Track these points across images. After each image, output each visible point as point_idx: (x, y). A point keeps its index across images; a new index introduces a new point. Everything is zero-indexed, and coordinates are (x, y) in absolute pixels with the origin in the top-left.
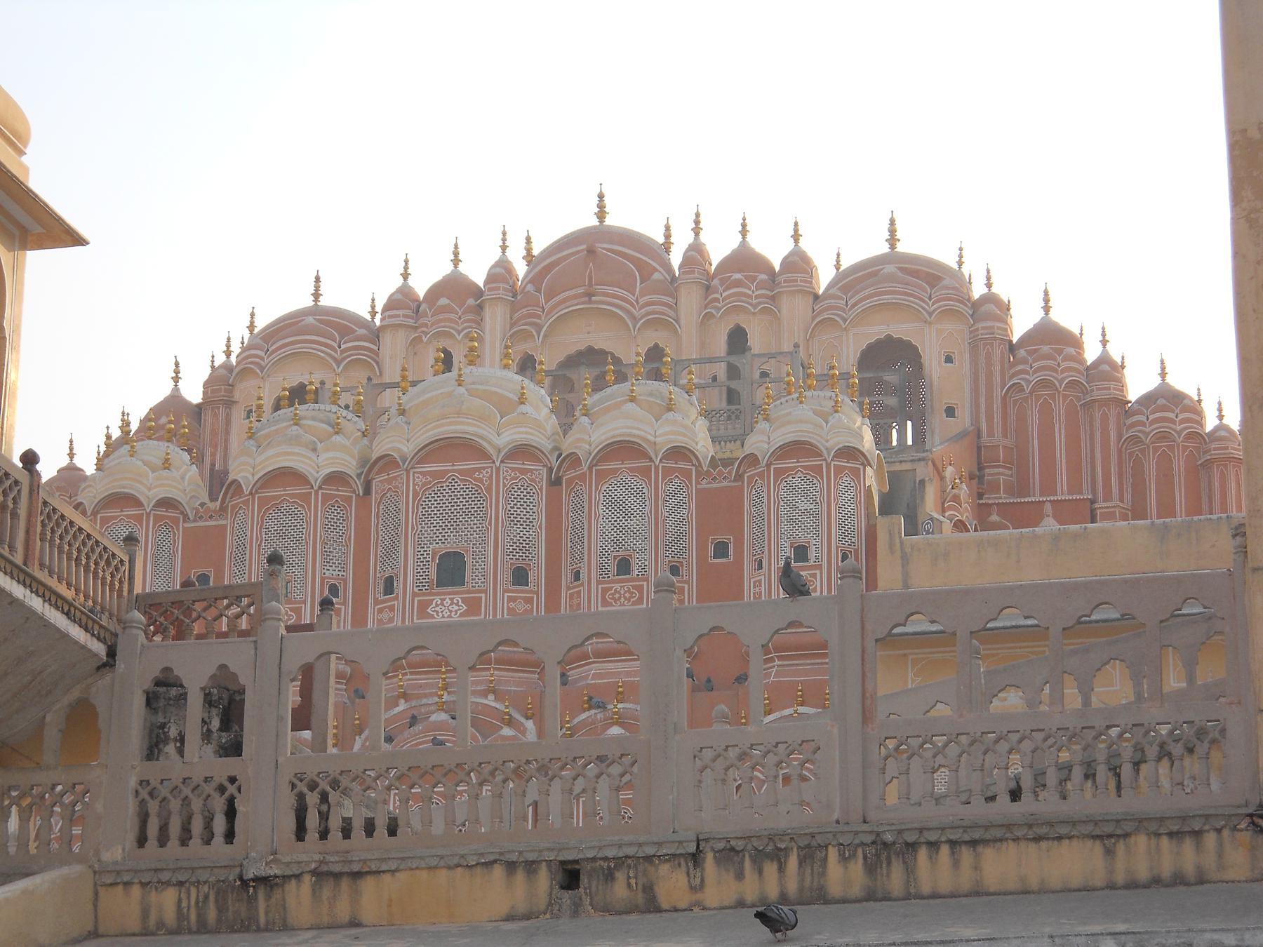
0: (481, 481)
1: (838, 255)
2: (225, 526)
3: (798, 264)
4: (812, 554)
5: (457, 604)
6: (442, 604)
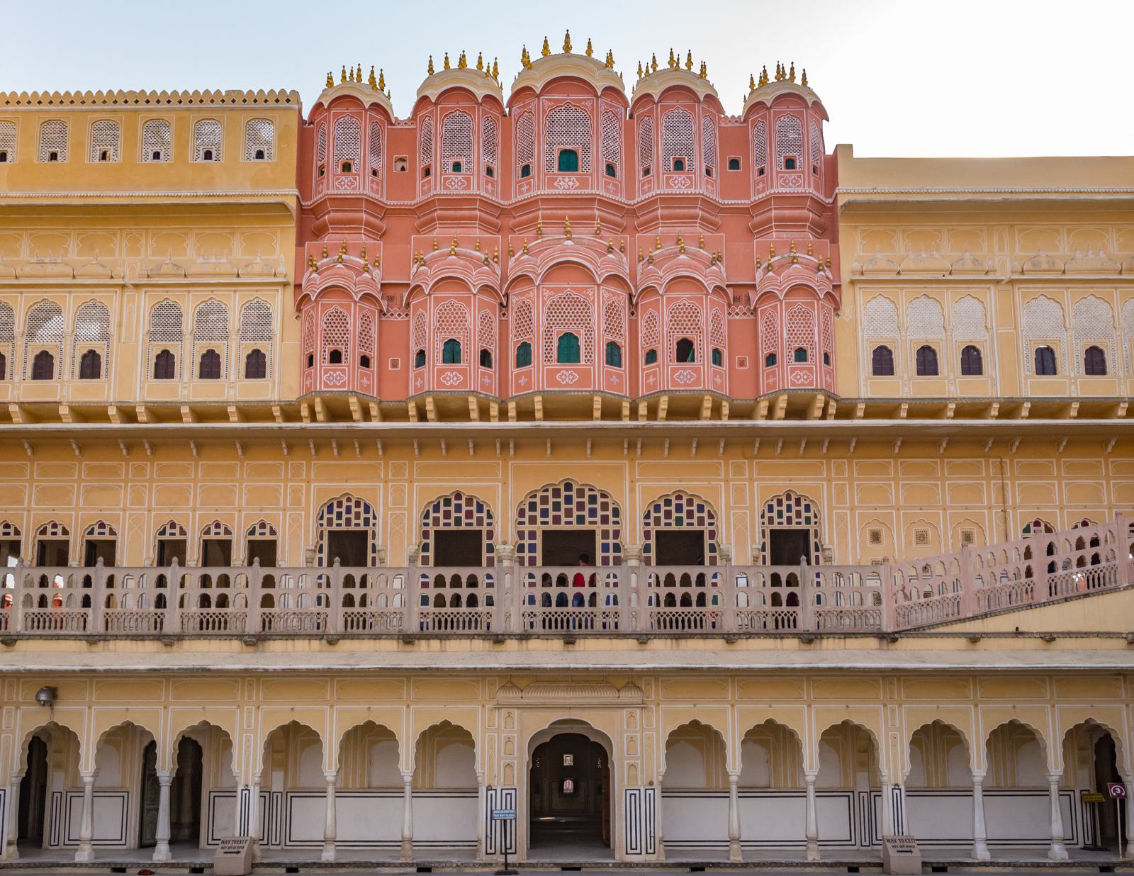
0: (587, 107)
5: (573, 181)
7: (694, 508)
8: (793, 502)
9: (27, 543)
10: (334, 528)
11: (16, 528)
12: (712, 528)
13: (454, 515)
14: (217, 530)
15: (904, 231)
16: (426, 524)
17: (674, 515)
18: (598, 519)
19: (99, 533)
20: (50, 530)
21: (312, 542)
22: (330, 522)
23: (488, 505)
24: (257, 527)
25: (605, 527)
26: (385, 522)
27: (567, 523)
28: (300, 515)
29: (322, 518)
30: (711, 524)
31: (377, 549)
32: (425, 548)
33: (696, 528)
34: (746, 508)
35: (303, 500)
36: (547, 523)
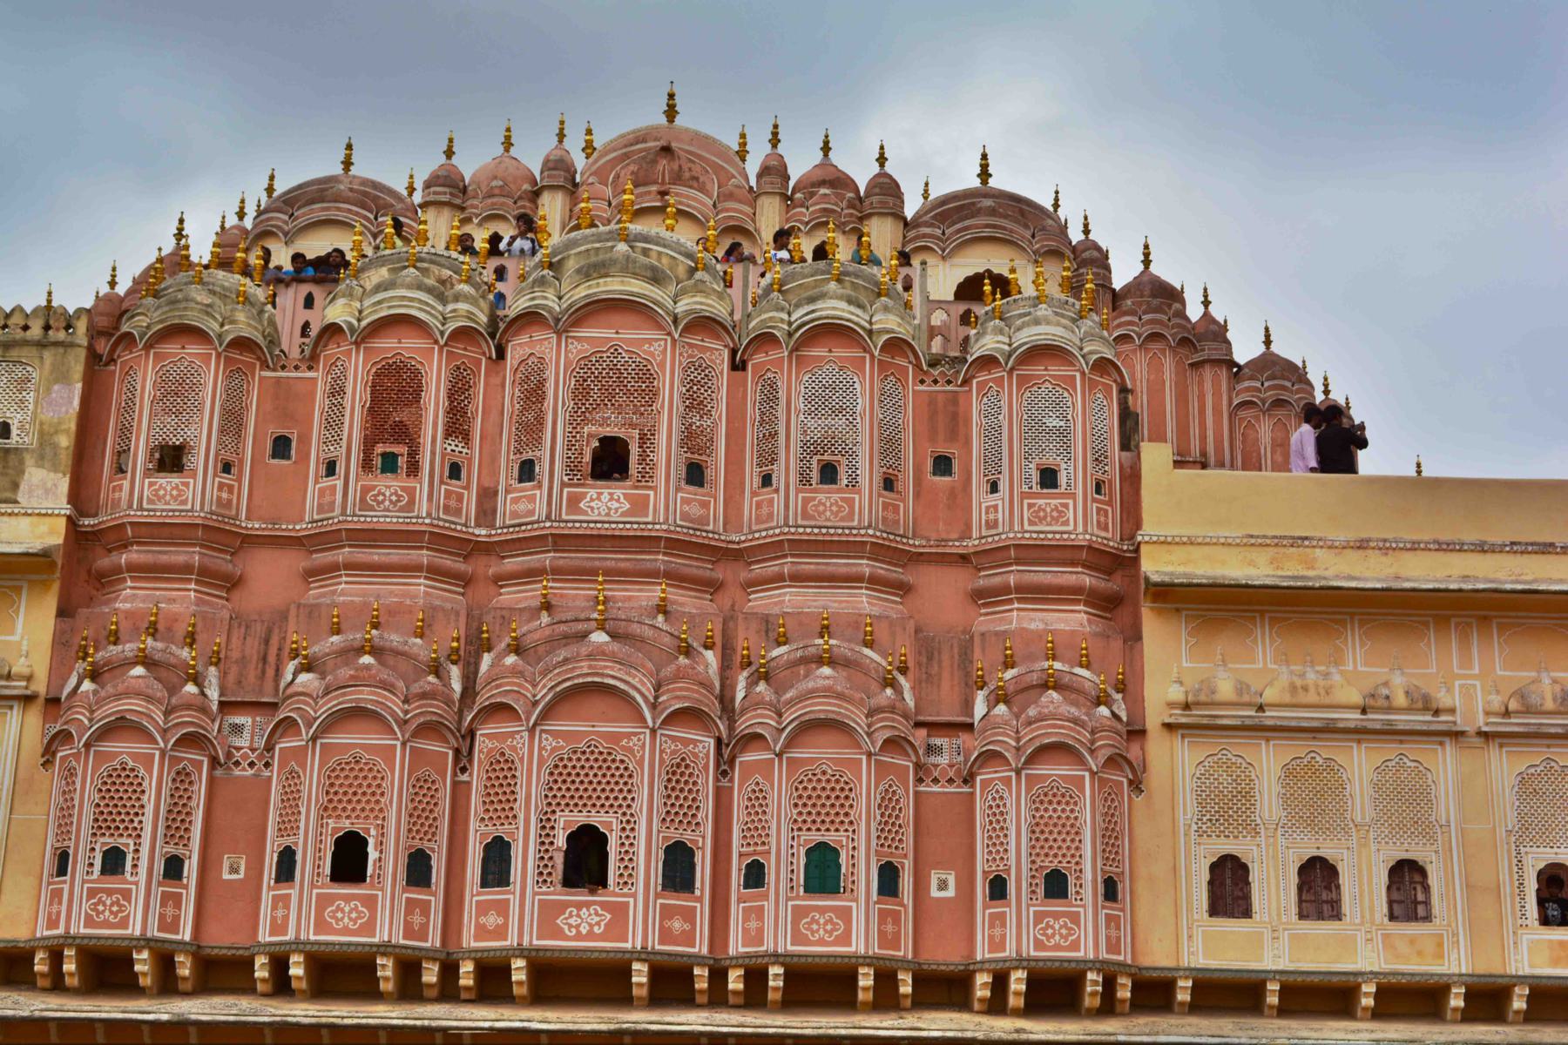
0: (652, 354)
1: (927, 184)
2: (314, 379)
3: (886, 188)
4: (1062, 479)
5: (618, 500)
6: (599, 499)
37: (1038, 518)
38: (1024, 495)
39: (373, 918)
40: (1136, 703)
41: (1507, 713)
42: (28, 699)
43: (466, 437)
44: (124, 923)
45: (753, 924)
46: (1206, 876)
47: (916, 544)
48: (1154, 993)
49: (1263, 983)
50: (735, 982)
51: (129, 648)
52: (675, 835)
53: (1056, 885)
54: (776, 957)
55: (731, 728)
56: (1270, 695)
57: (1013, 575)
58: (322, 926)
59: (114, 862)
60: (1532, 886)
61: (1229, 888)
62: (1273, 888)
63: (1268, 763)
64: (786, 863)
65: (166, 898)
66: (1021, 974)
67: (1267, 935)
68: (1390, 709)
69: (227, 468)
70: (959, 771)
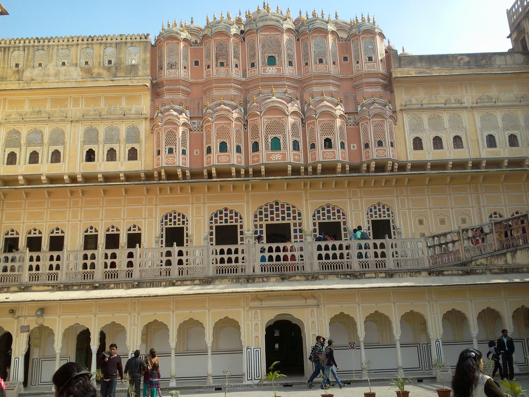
4: (373, 59)
7: (336, 211)
8: (381, 207)
9: (22, 239)
10: (168, 226)
11: (17, 232)
12: (344, 220)
13: (224, 218)
14: (113, 229)
15: (423, 86)
16: (212, 223)
17: (327, 215)
18: (291, 218)
19: (56, 233)
20: (33, 232)
21: (158, 232)
22: (166, 223)
23: (240, 213)
24: (132, 227)
25: (295, 221)
26: (192, 223)
27: (277, 220)
28: (153, 221)
29: (162, 222)
30: (343, 218)
31: (189, 235)
32: (211, 234)
33: (337, 220)
34: (360, 211)
35: (154, 214)
36: (268, 220)
37: (369, 67)
38: (365, 63)
39: (230, 159)
40: (394, 106)
41: (477, 103)
42: (146, 119)
43: (238, 59)
44: (174, 163)
45: (313, 156)
46: (412, 142)
47: (341, 76)
48: (402, 167)
49: (427, 163)
50: (310, 169)
51: (167, 107)
52: (294, 139)
53: (380, 144)
54: (319, 162)
55: (305, 117)
56: (424, 102)
57: (365, 80)
58: (218, 161)
59: (171, 151)
60: (485, 139)
61: (418, 144)
62: (427, 143)
63: (425, 117)
64: (320, 143)
65: (183, 158)
66: (374, 163)
67: (427, 153)
68: (451, 103)
69: (185, 68)
70: (356, 123)
